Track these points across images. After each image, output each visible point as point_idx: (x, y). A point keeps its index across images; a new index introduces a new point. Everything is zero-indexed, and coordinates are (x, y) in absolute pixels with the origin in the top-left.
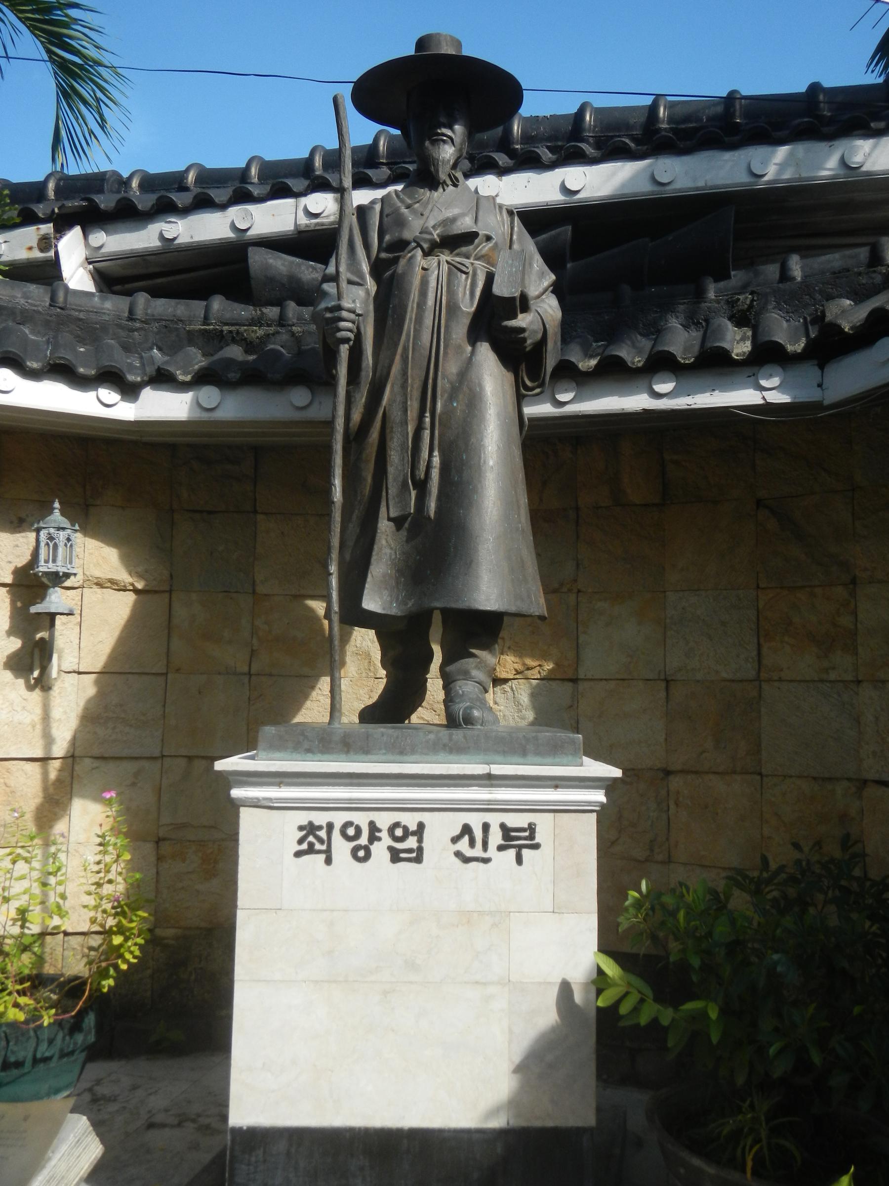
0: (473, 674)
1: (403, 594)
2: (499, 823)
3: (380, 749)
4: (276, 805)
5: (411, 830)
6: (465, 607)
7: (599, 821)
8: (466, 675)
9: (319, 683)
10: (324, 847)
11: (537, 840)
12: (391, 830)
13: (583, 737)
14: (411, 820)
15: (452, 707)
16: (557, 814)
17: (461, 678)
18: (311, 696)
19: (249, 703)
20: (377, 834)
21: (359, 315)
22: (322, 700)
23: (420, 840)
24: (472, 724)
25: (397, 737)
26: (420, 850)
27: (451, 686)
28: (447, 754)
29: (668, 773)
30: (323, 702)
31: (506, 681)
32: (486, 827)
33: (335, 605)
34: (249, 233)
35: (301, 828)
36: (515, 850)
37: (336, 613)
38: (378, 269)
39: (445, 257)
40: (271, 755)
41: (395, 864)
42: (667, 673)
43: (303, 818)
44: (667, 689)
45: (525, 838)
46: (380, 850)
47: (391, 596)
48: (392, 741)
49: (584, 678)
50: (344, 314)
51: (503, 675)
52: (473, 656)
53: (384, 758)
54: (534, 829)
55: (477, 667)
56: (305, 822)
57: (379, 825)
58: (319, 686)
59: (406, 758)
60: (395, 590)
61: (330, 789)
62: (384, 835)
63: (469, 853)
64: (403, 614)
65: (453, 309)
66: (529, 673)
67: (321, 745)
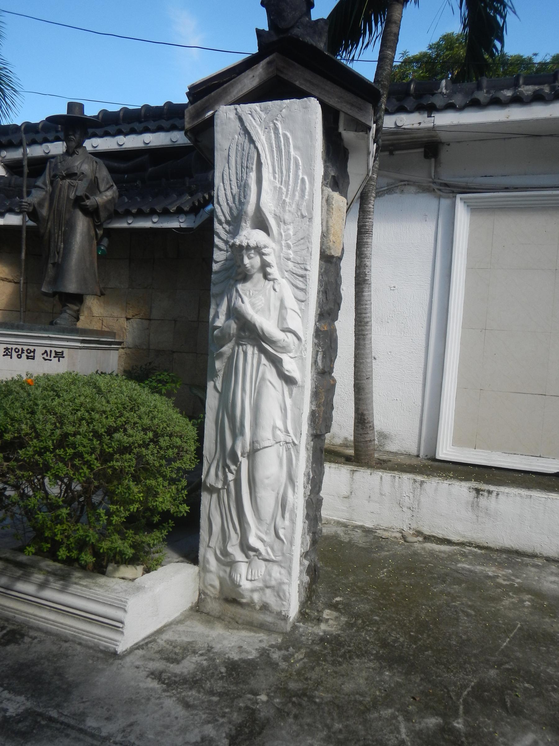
8: (65, 312)
14: (32, 348)
21: (29, 204)
23: (34, 354)
26: (34, 356)
29: (174, 352)
31: (129, 319)
32: (51, 351)
34: (50, 154)
35: (5, 349)
38: (52, 183)
39: (68, 181)
43: (5, 346)
46: (24, 356)
50: (24, 204)
51: (129, 317)
62: (25, 352)
63: (47, 358)
65: (68, 197)
66: (136, 317)
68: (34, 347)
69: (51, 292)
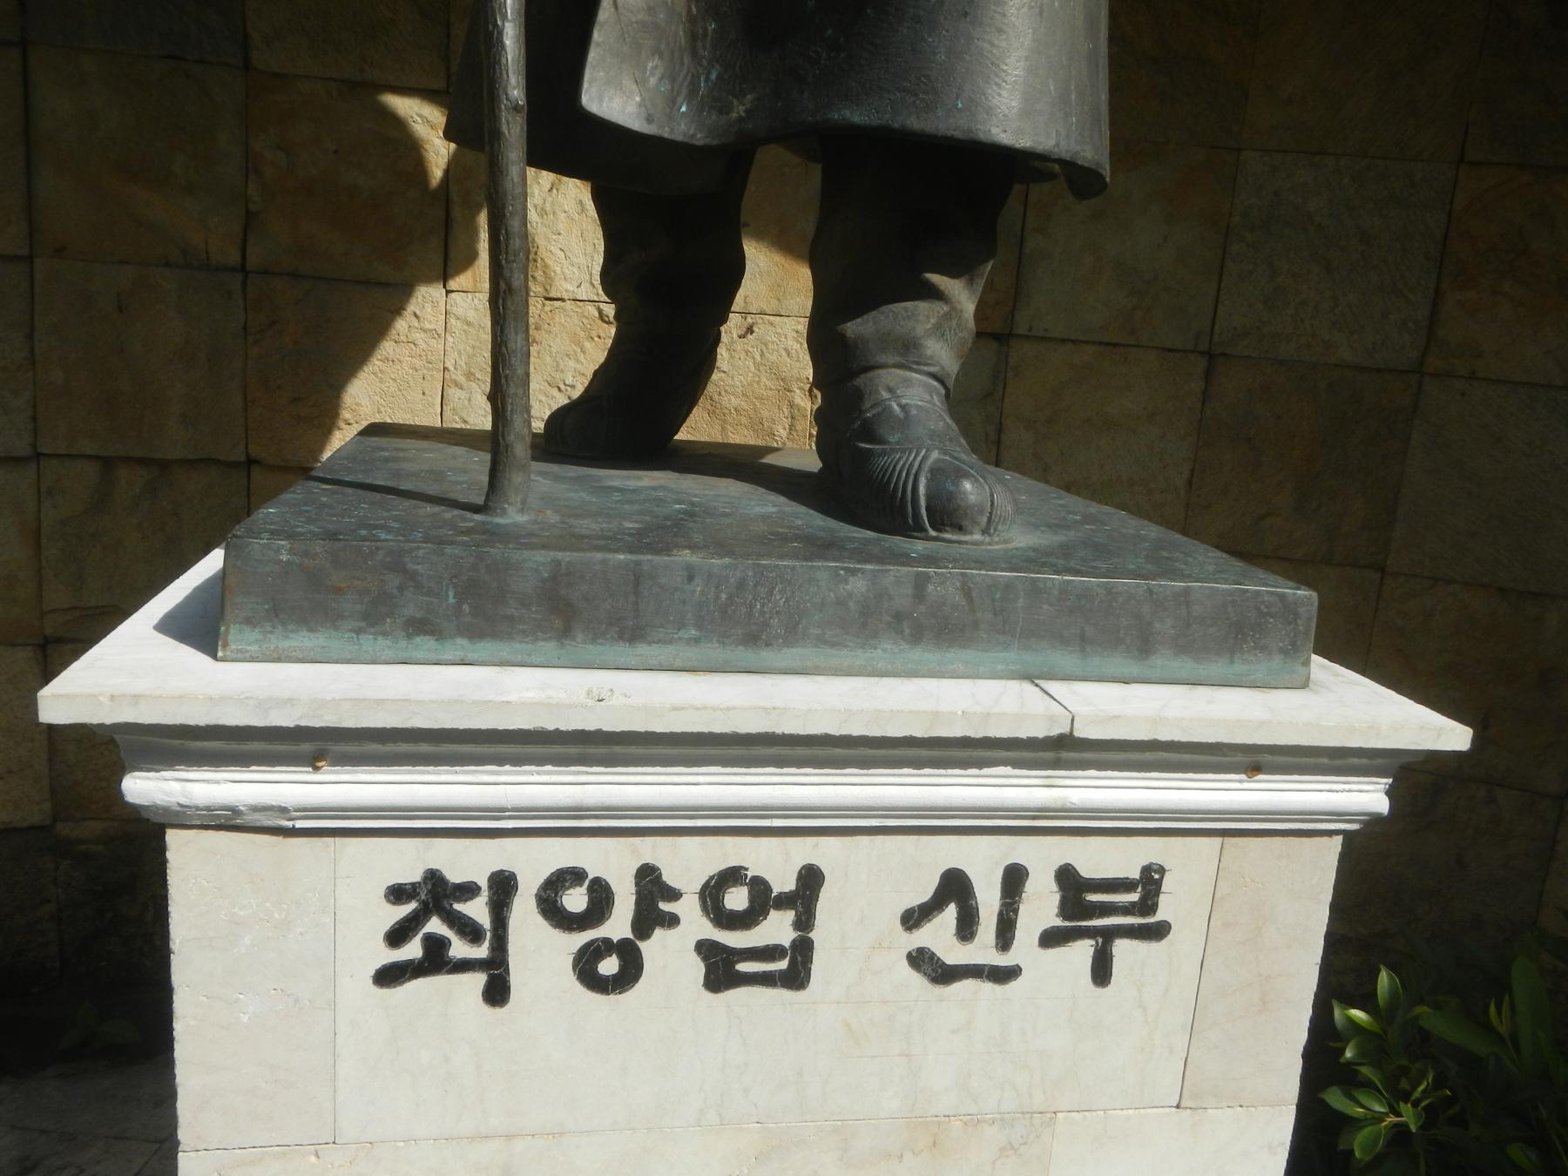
0: (929, 352)
1: (713, 76)
2: (1056, 867)
3: (681, 626)
4: (300, 824)
5: (776, 891)
6: (950, 133)
7: (1344, 858)
9: (413, 301)
10: (482, 952)
11: (1160, 916)
12: (712, 894)
13: (1320, 597)
15: (882, 461)
16: (1230, 841)
17: (891, 360)
18: (394, 332)
19: (245, 339)
20: (665, 906)
22: (420, 342)
23: (805, 922)
24: (960, 529)
25: (741, 585)
26: (802, 951)
27: (860, 381)
28: (905, 646)
30: (424, 346)
32: (1014, 879)
33: (513, 80)
35: (397, 894)
36: (1093, 942)
37: (516, 108)
40: (278, 642)
41: (720, 995)
42: (1216, 339)
44: (1208, 375)
45: (1127, 910)
47: (673, 80)
48: (724, 596)
49: (1027, 333)
52: (934, 294)
53: (691, 654)
54: (1159, 883)
55: (938, 330)
56: (415, 876)
57: (669, 878)
58: (412, 307)
59: (767, 656)
60: (687, 59)
61: (506, 773)
62: (689, 909)
63: (954, 954)
64: (716, 142)
67: (466, 607)
68: (803, 852)
69: (682, 126)
